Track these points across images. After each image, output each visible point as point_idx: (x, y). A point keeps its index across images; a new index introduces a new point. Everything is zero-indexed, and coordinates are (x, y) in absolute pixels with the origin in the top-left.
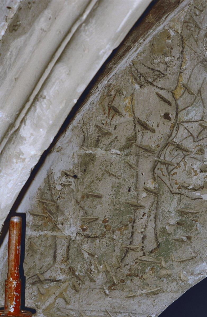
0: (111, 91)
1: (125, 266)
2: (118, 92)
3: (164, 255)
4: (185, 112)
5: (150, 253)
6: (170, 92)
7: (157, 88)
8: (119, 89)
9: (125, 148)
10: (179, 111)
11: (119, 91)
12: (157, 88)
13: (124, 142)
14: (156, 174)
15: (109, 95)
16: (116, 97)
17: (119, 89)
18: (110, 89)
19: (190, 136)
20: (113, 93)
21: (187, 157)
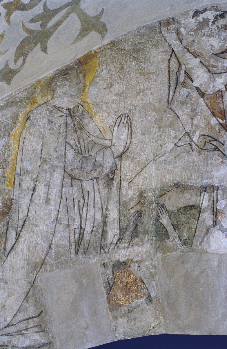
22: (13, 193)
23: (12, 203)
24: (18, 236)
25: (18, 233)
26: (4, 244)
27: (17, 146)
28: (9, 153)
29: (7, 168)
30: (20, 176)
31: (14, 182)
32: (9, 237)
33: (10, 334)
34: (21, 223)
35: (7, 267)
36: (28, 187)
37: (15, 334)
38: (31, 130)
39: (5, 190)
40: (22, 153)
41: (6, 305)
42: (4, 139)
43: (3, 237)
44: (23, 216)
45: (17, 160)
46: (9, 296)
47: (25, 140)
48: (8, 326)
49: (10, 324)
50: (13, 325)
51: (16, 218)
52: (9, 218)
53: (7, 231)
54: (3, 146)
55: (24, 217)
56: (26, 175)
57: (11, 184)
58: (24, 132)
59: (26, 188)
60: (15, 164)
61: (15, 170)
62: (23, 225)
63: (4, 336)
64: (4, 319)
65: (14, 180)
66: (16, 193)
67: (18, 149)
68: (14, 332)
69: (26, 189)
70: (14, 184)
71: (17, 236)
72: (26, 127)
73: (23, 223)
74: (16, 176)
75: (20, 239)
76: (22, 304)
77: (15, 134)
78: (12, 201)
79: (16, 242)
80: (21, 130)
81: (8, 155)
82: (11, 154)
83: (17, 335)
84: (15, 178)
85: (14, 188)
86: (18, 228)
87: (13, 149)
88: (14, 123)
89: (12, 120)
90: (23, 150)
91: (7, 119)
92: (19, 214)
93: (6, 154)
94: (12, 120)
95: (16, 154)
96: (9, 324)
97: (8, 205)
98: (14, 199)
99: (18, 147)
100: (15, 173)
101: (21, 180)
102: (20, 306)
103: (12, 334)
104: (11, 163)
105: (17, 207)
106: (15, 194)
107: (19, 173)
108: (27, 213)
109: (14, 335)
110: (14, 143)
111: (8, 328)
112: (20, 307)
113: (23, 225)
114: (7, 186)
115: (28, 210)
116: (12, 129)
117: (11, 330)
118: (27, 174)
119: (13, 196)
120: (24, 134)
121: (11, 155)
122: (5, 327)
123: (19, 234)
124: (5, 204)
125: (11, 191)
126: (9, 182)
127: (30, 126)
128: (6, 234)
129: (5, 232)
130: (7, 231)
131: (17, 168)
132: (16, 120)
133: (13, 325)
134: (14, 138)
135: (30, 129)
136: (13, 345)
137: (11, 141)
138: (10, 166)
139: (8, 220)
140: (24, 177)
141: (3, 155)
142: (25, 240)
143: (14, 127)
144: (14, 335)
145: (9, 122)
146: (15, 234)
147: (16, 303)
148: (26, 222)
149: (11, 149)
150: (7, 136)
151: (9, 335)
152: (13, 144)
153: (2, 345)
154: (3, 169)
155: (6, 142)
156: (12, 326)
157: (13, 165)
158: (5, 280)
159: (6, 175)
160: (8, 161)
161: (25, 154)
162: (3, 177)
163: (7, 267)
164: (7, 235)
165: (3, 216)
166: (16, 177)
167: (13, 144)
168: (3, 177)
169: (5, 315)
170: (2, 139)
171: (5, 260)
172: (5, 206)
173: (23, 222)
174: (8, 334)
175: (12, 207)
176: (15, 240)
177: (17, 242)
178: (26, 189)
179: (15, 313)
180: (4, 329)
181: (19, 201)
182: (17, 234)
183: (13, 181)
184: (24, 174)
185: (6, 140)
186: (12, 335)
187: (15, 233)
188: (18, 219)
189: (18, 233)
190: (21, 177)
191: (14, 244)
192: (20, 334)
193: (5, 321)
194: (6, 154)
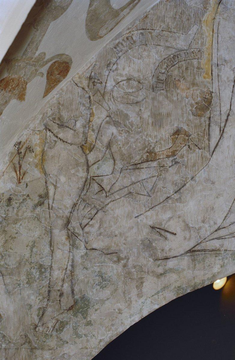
0: (21, 149)
1: (43, 324)
2: (28, 150)
3: (82, 311)
4: (96, 166)
5: (68, 311)
6: (80, 147)
7: (67, 143)
8: (29, 146)
9: (37, 205)
10: (90, 165)
11: (29, 148)
12: (67, 143)
13: (37, 200)
14: (69, 230)
15: (19, 153)
16: (26, 154)
17: (29, 146)
18: (20, 147)
19: (102, 190)
20: (23, 151)
21: (100, 211)
22: (212, 86)
23: (212, 97)
24: (222, 132)
25: (222, 129)
26: (207, 142)
27: (211, 33)
28: (203, 41)
29: (201, 58)
30: (218, 66)
31: (212, 74)
32: (212, 134)
33: (222, 238)
34: (224, 118)
35: (212, 166)
36: (228, 78)
37: (227, 237)
38: (225, 15)
39: (202, 82)
40: (218, 41)
41: (214, 207)
42: (195, 26)
43: (205, 134)
44: (225, 111)
45: (213, 49)
46: (217, 197)
47: (219, 27)
48: (219, 229)
49: (221, 227)
50: (224, 228)
51: (218, 113)
52: (210, 113)
53: (209, 127)
54: (195, 34)
55: (227, 111)
56: (224, 65)
57: (209, 76)
58: (218, 17)
59: (225, 79)
60: (211, 54)
61: (212, 60)
62: (227, 120)
63: (216, 240)
64: (214, 222)
65: (212, 71)
66: (215, 85)
67: (213, 37)
68: (226, 235)
69: (226, 81)
70: (212, 75)
71: (222, 132)
72: (219, 12)
73: (226, 118)
74: (213, 66)
75: (224, 135)
76: (232, 205)
77: (207, 21)
78: (212, 95)
79: (220, 138)
80: (214, 15)
81: (202, 44)
82: (206, 42)
83: (229, 238)
84: (212, 68)
85: (212, 79)
86: (221, 123)
87: (207, 37)
88: (205, 8)
89: (202, 5)
90: (218, 38)
91: (196, 3)
92: (220, 109)
93: (200, 42)
94: (202, 5)
95: (211, 42)
96: (219, 227)
97: (207, 99)
98: (214, 91)
99: (213, 35)
100: (212, 63)
101: (220, 70)
102: (231, 207)
103: (223, 237)
104: (206, 52)
105: (219, 101)
106: (214, 86)
107: (217, 63)
108: (230, 107)
109: (226, 238)
110: (207, 30)
111: (218, 231)
112: (230, 209)
113: (227, 120)
114: (205, 78)
115: (231, 103)
116: (203, 15)
117: (222, 233)
118: (225, 64)
119: (212, 88)
120: (217, 20)
121: (205, 43)
122: (216, 231)
123: (223, 130)
124: (204, 97)
125: (210, 84)
126: (206, 74)
127: (223, 11)
128: (209, 131)
129: (207, 129)
130: (209, 127)
131: (213, 58)
132: (207, 4)
133: (224, 228)
134: (207, 25)
135: (223, 14)
136: (225, 248)
137: (204, 28)
138: (205, 56)
139: (209, 114)
140: (222, 69)
141: (196, 44)
142: (231, 136)
143: (205, 12)
144: (226, 238)
145: (199, 7)
146: (219, 130)
147: (226, 204)
148: (229, 117)
149: (204, 36)
150: (199, 22)
151: (220, 239)
152: (206, 32)
153: (214, 250)
154: (198, 59)
155: (198, 29)
156: (223, 229)
157: (209, 54)
158: (212, 180)
159: (202, 66)
160: (203, 50)
161: (221, 42)
162: (199, 68)
163: (212, 166)
164: (210, 131)
165: (204, 112)
166: (213, 68)
167: (206, 32)
168: (199, 68)
169: (215, 218)
170: (193, 26)
171: (210, 159)
172: (204, 100)
173: (226, 116)
174: (220, 237)
175: (212, 100)
176: (220, 137)
177: (221, 138)
178: (226, 81)
179: (225, 215)
180: (215, 233)
181: (219, 93)
182: (220, 130)
183: (210, 72)
184: (222, 64)
185: (198, 27)
186: (223, 238)
187: (219, 129)
188: (221, 114)
189: (222, 129)
190: (219, 67)
191: (219, 141)
192: (233, 237)
193: (215, 223)
194: (200, 42)
